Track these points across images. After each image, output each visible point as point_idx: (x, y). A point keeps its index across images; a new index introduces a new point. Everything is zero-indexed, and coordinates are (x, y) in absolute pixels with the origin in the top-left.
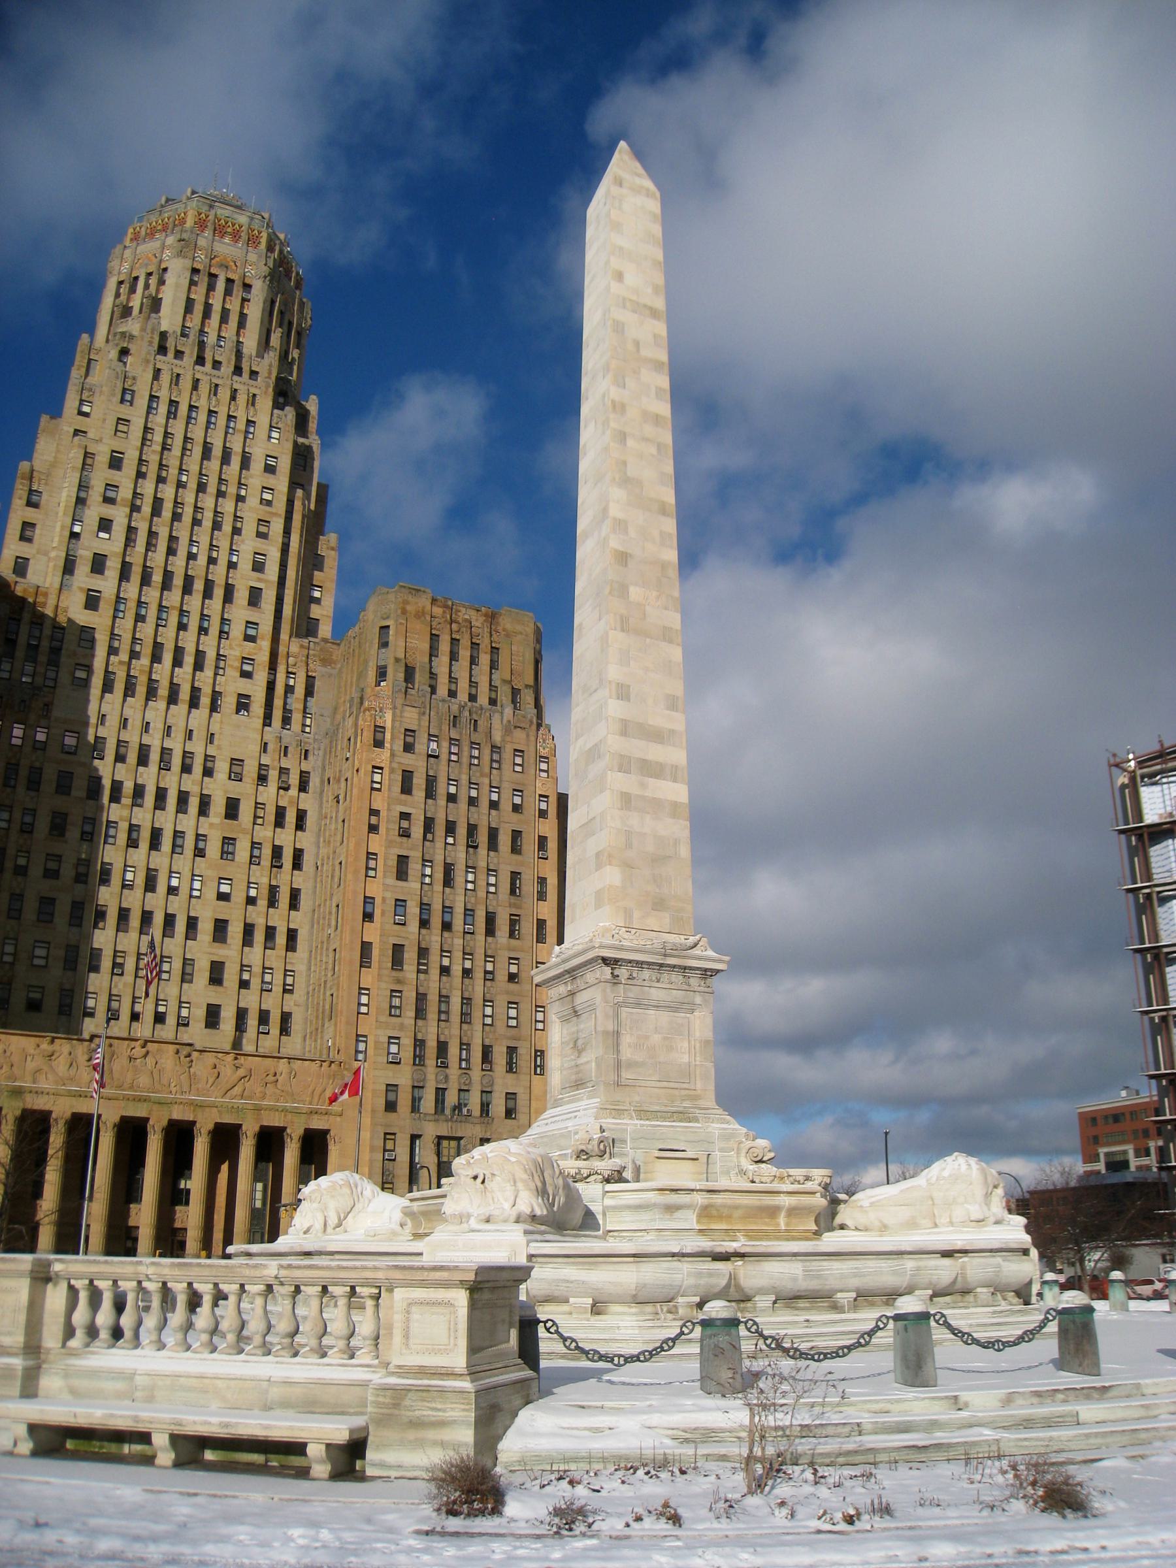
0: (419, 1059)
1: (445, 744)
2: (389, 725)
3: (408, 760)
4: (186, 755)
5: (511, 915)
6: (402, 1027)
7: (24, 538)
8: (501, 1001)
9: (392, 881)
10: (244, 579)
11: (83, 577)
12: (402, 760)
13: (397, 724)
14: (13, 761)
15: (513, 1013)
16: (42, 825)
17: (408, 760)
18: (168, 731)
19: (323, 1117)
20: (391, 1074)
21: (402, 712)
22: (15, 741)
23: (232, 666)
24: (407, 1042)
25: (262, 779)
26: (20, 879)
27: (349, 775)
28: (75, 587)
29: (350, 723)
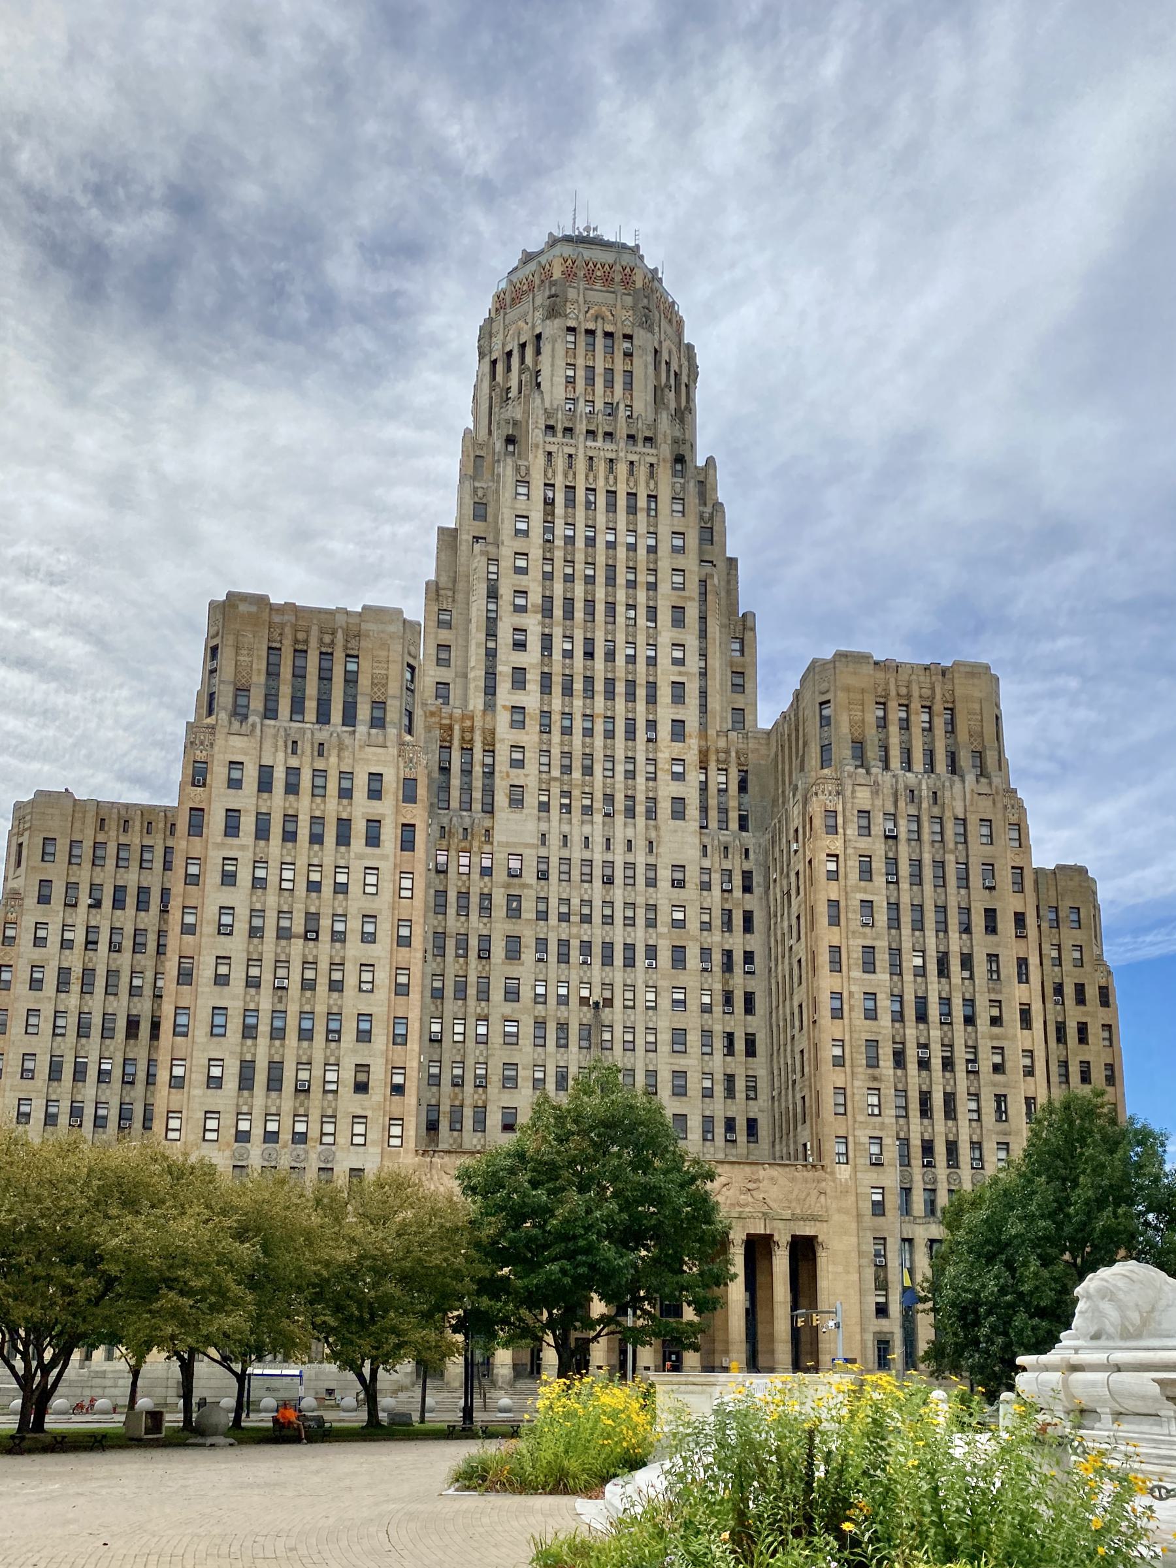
0: (905, 1160)
3: (864, 844)
4: (630, 866)
6: (883, 1126)
7: (442, 662)
9: (857, 973)
11: (505, 695)
16: (498, 950)
17: (864, 844)
19: (808, 1223)
20: (875, 1176)
22: (462, 870)
24: (890, 1142)
27: (800, 867)
28: (499, 707)
29: (796, 812)
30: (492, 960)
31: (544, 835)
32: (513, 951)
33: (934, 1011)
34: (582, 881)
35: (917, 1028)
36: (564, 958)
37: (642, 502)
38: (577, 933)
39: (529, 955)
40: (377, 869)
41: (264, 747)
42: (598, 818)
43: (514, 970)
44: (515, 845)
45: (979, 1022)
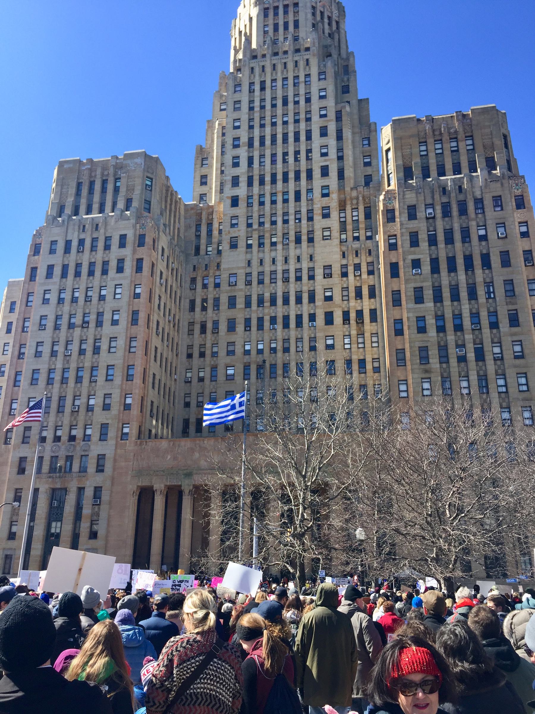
1: (439, 209)
2: (397, 206)
5: (508, 311)
8: (511, 373)
9: (412, 305)
10: (318, 162)
12: (408, 226)
13: (402, 204)
14: (205, 297)
15: (523, 381)
16: (223, 327)
17: (413, 225)
18: (286, 260)
21: (404, 195)
23: (317, 214)
25: (345, 275)
26: (215, 359)
30: (220, 334)
31: (249, 261)
32: (232, 326)
33: (467, 322)
34: (271, 283)
35: (455, 335)
36: (260, 326)
37: (302, 79)
38: (267, 312)
39: (240, 328)
40: (121, 285)
41: (69, 231)
42: (279, 247)
43: (232, 338)
44: (232, 268)
45: (501, 325)
